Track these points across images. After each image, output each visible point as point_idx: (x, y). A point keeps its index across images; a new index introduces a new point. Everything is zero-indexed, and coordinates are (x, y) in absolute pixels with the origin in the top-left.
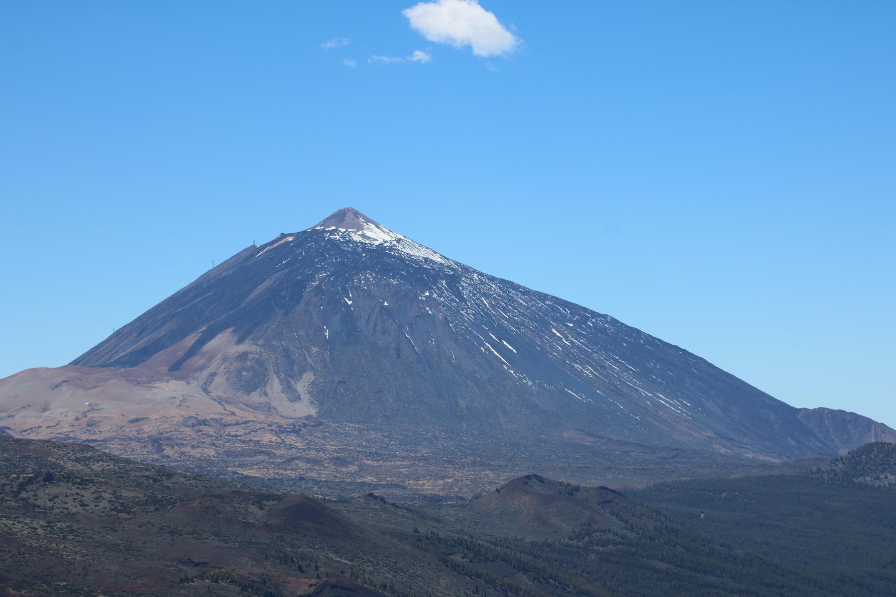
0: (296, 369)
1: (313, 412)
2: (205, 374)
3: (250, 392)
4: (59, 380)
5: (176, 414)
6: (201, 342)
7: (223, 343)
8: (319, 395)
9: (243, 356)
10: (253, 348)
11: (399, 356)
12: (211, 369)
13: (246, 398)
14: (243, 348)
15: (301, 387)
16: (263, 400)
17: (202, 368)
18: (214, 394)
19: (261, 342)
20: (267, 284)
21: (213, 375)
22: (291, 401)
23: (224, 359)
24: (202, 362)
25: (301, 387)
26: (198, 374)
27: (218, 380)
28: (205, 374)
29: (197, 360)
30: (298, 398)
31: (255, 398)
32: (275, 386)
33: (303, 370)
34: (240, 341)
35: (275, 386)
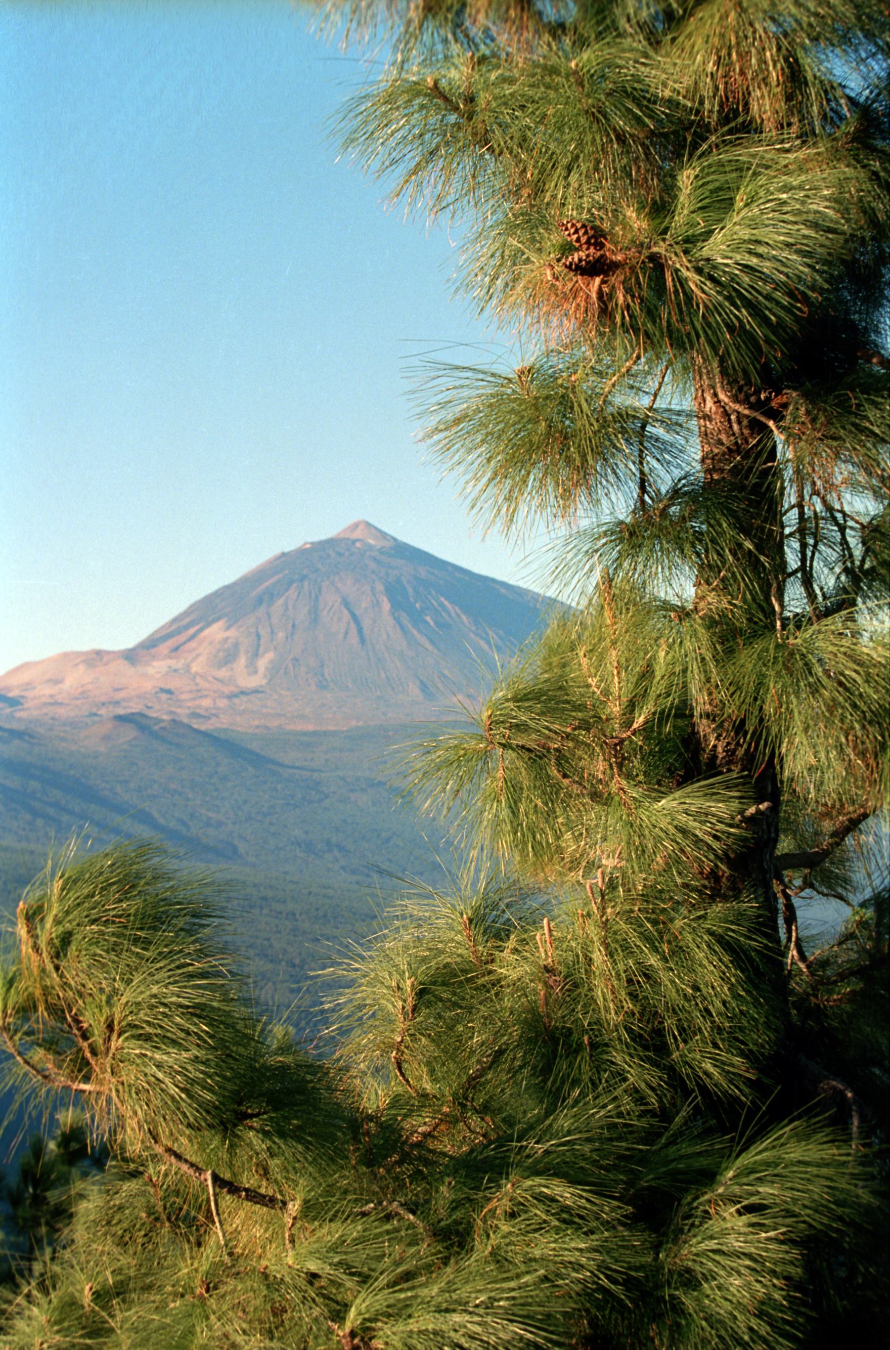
1: (264, 682)
4: (79, 660)
5: (149, 686)
6: (201, 630)
7: (216, 631)
8: (274, 670)
11: (345, 637)
15: (263, 663)
17: (194, 649)
21: (198, 655)
22: (249, 674)
23: (211, 643)
25: (263, 663)
27: (201, 659)
28: (194, 655)
29: (193, 644)
30: (256, 672)
31: (223, 673)
32: (242, 661)
33: (267, 651)
34: (228, 628)
35: (242, 661)
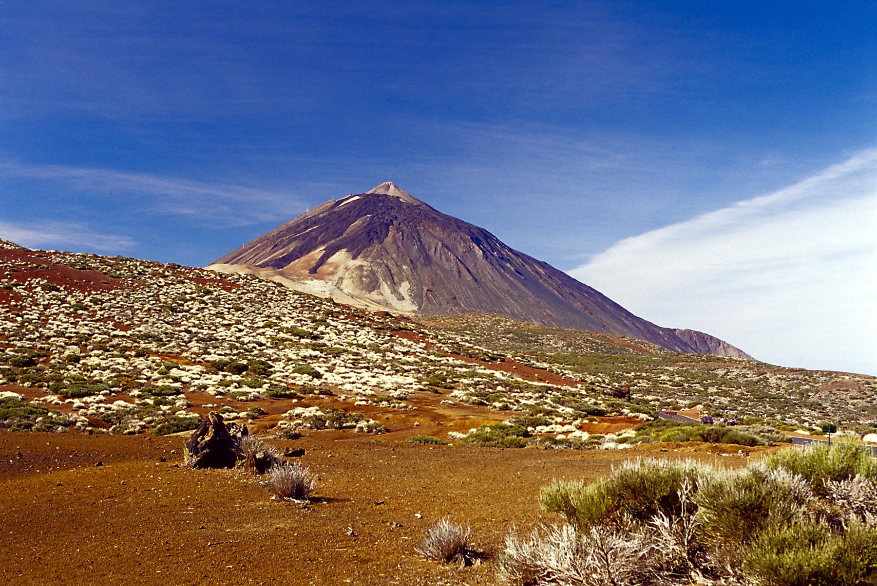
0: (396, 279)
2: (336, 278)
3: (370, 292)
8: (417, 297)
9: (361, 267)
10: (365, 263)
12: (340, 273)
13: (368, 295)
14: (359, 262)
16: (380, 298)
18: (345, 291)
19: (369, 259)
20: (358, 222)
21: (341, 279)
24: (331, 269)
26: (331, 277)
28: (336, 278)
31: (374, 295)
32: (385, 288)
34: (354, 258)
